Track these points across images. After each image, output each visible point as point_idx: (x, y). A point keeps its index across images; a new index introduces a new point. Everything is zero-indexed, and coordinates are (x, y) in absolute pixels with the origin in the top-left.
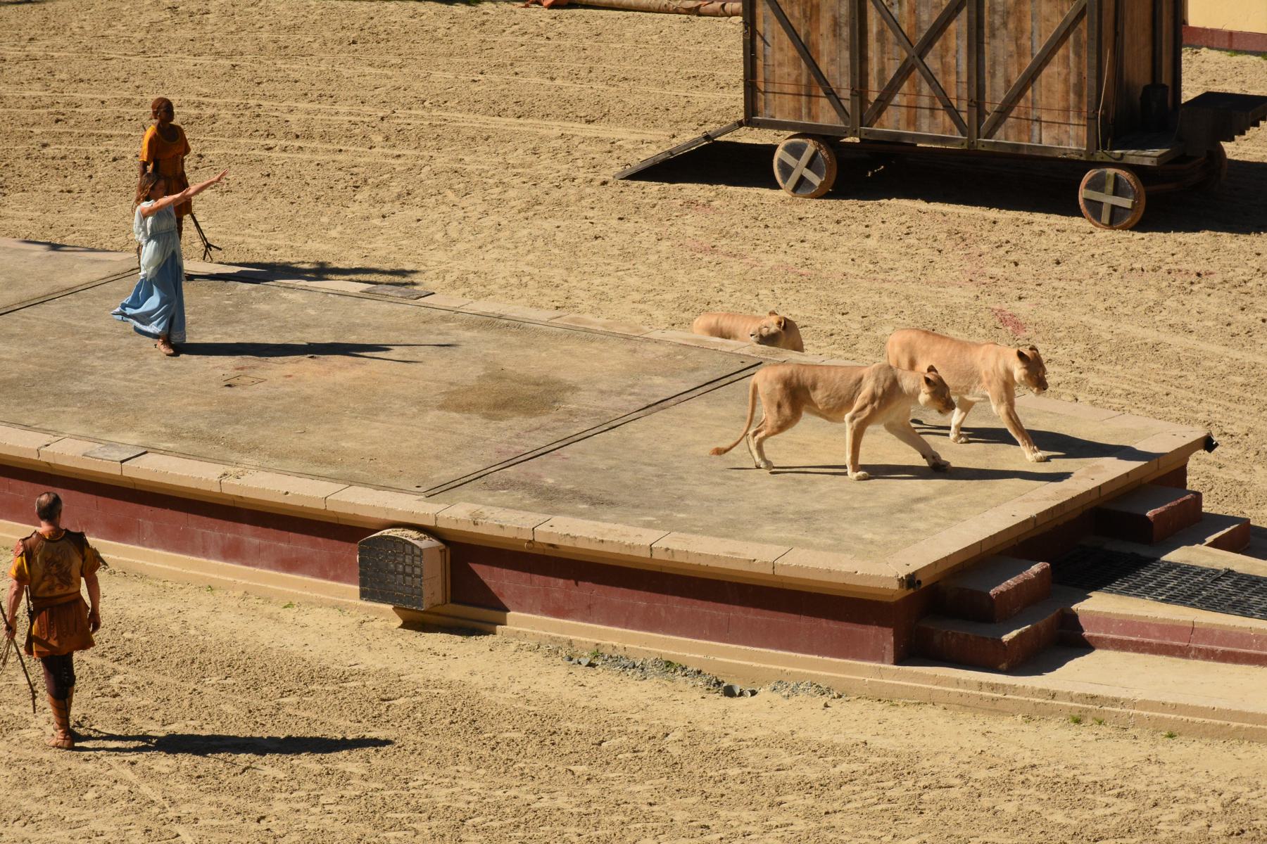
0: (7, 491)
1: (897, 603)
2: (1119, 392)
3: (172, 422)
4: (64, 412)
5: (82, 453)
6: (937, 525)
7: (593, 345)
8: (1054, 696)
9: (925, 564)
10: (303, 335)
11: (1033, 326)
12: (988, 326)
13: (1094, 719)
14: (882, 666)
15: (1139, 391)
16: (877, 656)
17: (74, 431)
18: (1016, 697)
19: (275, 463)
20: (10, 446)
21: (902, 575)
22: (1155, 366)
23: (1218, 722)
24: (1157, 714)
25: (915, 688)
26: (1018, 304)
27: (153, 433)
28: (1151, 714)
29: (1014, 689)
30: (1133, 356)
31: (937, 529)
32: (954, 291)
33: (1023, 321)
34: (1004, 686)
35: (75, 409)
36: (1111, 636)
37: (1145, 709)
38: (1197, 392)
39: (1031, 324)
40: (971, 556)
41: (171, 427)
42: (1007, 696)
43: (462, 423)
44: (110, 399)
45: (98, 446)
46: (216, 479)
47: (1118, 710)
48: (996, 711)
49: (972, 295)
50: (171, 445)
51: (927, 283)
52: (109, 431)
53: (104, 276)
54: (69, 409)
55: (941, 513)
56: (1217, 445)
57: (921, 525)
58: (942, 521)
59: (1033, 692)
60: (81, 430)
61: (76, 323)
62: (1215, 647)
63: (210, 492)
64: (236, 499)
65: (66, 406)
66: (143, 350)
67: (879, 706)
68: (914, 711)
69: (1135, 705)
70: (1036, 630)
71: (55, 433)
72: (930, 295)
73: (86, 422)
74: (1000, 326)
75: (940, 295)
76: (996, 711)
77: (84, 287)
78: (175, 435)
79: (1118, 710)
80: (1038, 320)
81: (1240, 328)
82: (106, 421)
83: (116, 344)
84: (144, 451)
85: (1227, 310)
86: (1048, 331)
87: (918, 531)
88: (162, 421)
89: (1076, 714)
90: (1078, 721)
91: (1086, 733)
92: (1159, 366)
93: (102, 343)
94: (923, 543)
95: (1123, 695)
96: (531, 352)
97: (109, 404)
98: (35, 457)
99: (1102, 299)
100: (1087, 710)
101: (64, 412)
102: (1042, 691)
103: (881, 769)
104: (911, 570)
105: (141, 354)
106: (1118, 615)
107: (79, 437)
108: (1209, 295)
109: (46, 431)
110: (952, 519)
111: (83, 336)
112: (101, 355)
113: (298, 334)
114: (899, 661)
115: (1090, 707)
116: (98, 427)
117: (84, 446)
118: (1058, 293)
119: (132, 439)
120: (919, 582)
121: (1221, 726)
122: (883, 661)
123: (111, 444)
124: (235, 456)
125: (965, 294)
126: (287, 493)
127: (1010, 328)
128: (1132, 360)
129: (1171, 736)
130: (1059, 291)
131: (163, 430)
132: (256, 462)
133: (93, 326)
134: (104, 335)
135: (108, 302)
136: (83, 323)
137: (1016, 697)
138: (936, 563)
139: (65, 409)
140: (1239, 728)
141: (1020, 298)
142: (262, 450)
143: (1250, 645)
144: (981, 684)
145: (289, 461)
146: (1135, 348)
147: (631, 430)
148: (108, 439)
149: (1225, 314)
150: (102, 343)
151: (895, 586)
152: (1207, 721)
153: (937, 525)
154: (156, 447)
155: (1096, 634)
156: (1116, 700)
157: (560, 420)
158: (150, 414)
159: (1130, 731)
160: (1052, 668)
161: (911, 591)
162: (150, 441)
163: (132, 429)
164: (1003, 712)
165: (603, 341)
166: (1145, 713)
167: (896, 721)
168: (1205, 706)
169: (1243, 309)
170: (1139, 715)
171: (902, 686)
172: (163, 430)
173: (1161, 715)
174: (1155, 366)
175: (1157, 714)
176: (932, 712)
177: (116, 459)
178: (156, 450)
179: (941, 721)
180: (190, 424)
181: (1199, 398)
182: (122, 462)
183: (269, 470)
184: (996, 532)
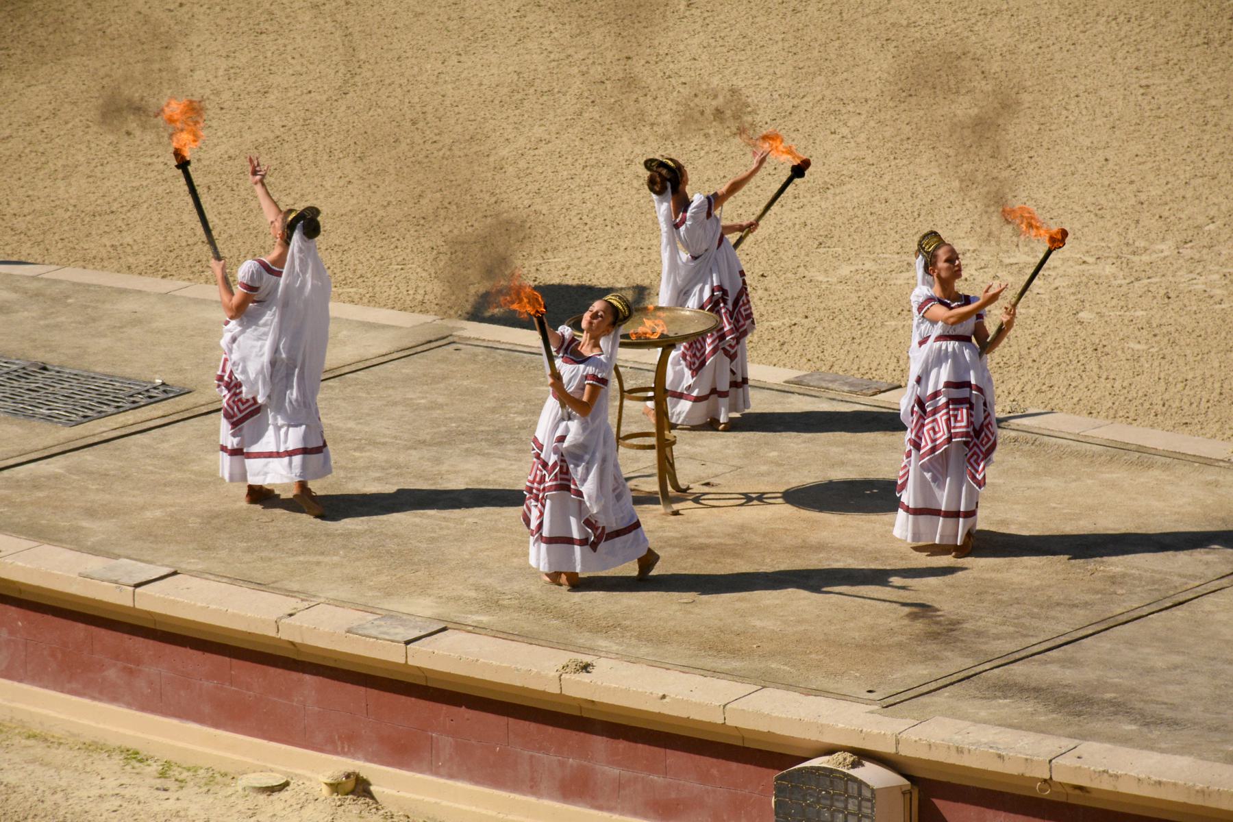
0: (227, 686)
3: (488, 581)
4: (318, 563)
5: (346, 627)
7: (1151, 472)
10: (694, 450)
17: (331, 595)
19: (644, 650)
20: (234, 615)
27: (457, 599)
35: (336, 559)
41: (486, 589)
43: (941, 593)
44: (392, 545)
45: (371, 617)
46: (553, 674)
50: (484, 619)
52: (389, 594)
53: (383, 351)
54: (326, 559)
60: (344, 592)
61: (341, 425)
63: (544, 692)
64: (585, 705)
65: (322, 554)
66: (444, 468)
71: (304, 595)
73: (354, 579)
77: (353, 368)
78: (492, 603)
82: (384, 578)
83: (402, 458)
84: (443, 626)
88: (471, 581)
93: (380, 456)
96: (1051, 483)
97: (388, 552)
98: (272, 633)
101: (318, 563)
105: (440, 474)
107: (339, 603)
109: (289, 593)
111: (349, 445)
112: (378, 475)
113: (687, 448)
116: (371, 588)
117: (353, 617)
119: (423, 607)
123: (390, 616)
124: (583, 639)
126: (664, 697)
131: (473, 594)
132: (615, 648)
133: (367, 429)
134: (384, 444)
135: (391, 392)
136: (351, 424)
139: (321, 558)
142: (625, 628)
145: (668, 647)
147: (1208, 607)
148: (386, 606)
150: (380, 456)
154: (462, 621)
157: (1097, 593)
158: (452, 570)
162: (451, 612)
163: (424, 590)
165: (1166, 467)
172: (473, 594)
177: (399, 638)
178: (460, 626)
180: (516, 586)
182: (407, 643)
183: (635, 660)
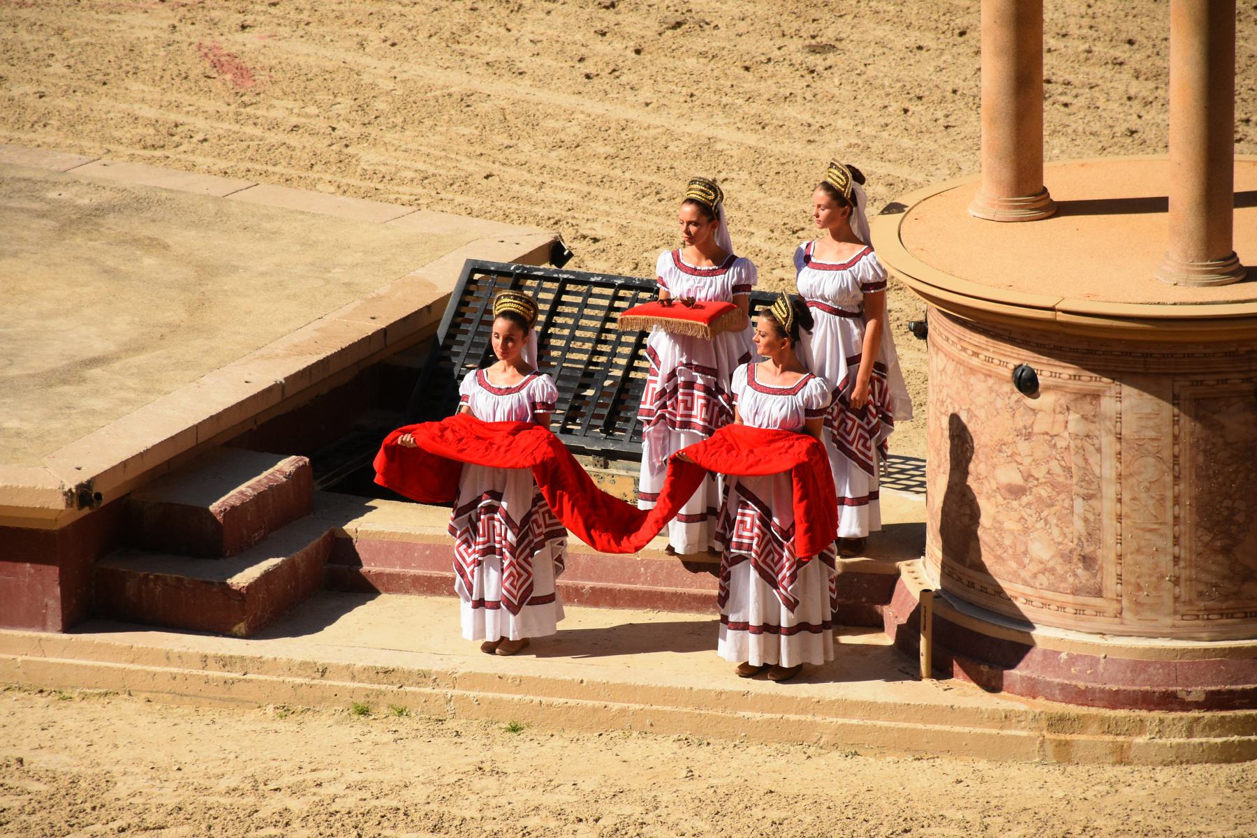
1: (63, 531)
2: (410, 174)
6: (125, 401)
8: (324, 672)
9: (107, 467)
11: (266, 73)
12: (192, 75)
13: (391, 706)
14: (43, 635)
15: (442, 171)
16: (35, 620)
18: (262, 677)
21: (71, 485)
22: (466, 131)
23: (590, 703)
24: (490, 695)
25: (99, 668)
26: (240, 37)
28: (482, 694)
29: (259, 663)
30: (430, 115)
31: (125, 409)
32: (137, 18)
33: (249, 65)
34: (242, 659)
36: (413, 572)
37: (472, 688)
38: (536, 171)
39: (263, 68)
40: (180, 451)
42: (248, 676)
47: (428, 690)
48: (232, 700)
49: (165, 24)
51: (91, 8)
55: (130, 383)
56: (570, 255)
57: (98, 403)
58: (132, 395)
59: (290, 668)
62: (580, 583)
67: (40, 700)
68: (99, 707)
69: (454, 680)
70: (291, 566)
72: (96, 26)
74: (213, 73)
75: (113, 26)
76: (232, 700)
79: (428, 690)
80: (274, 62)
81: (601, 65)
85: (578, 37)
86: (292, 79)
87: (93, 412)
89: (361, 701)
90: (364, 712)
91: (377, 731)
92: (472, 130)
94: (102, 432)
95: (435, 666)
99: (376, 23)
100: (380, 693)
102: (304, 665)
103: (47, 804)
104: (84, 477)
106: (422, 536)
108: (549, 13)
110: (147, 391)
114: (71, 626)
115: (383, 687)
118: (305, 16)
120: (98, 496)
121: (595, 710)
122: (44, 627)
125: (154, 23)
127: (228, 77)
128: (428, 123)
129: (515, 729)
130: (306, 13)
137: (262, 677)
138: (124, 464)
140: (623, 712)
141: (243, 27)
143: (636, 577)
144: (205, 659)
146: (432, 103)
149: (575, 43)
151: (59, 503)
152: (572, 702)
153: (125, 401)
155: (388, 570)
156: (424, 675)
159: (450, 724)
160: (315, 625)
161: (86, 511)
164: (243, 702)
166: (472, 694)
167: (70, 724)
168: (568, 678)
169: (604, 34)
170: (463, 698)
171: (77, 667)
173: (497, 695)
174: (466, 131)
175: (490, 695)
176: (127, 707)
179: (143, 721)
181: (539, 180)
184: (220, 409)
